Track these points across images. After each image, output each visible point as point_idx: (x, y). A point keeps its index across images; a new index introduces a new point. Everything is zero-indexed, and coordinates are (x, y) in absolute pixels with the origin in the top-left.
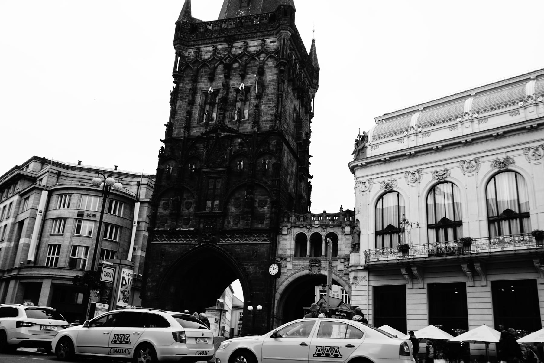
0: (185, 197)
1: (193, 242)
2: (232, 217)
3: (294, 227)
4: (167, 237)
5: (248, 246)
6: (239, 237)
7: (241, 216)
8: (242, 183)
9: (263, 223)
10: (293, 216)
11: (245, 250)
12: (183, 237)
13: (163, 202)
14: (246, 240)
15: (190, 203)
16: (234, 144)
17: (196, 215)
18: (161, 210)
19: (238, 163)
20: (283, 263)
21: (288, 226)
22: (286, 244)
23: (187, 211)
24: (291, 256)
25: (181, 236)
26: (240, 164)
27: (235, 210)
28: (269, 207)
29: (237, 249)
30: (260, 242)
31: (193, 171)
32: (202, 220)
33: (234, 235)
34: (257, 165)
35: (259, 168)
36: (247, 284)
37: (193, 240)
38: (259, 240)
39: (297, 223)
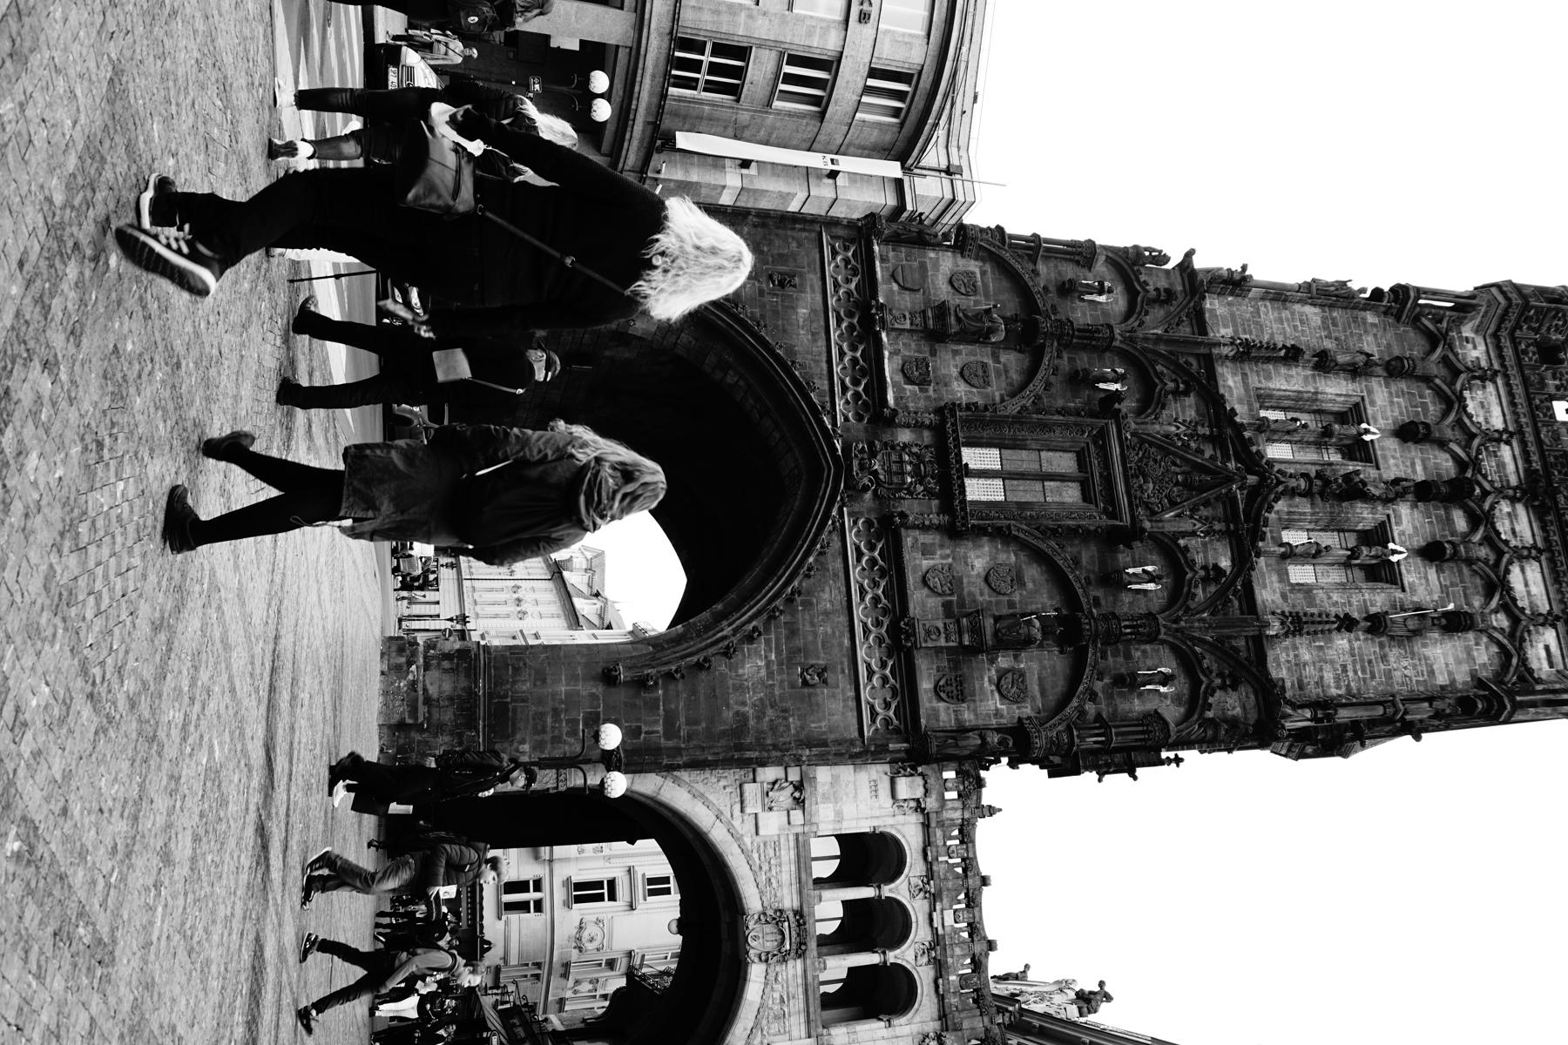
0: (1002, 360)
1: (840, 404)
2: (950, 560)
3: (923, 824)
4: (849, 294)
5: (846, 642)
6: (876, 600)
7: (954, 598)
8: (1080, 591)
9: (941, 699)
10: (967, 815)
11: (829, 630)
12: (854, 361)
13: (977, 271)
14: (866, 631)
15: (987, 383)
16: (1211, 541)
17: (946, 411)
18: (946, 263)
19: (1150, 568)
20: (784, 797)
21: (928, 800)
22: (856, 796)
23: (954, 372)
24: (812, 824)
25: (858, 354)
26: (1152, 578)
27: (974, 573)
28: (1002, 716)
29: (829, 597)
30: (865, 695)
31: (1102, 386)
32: (926, 434)
33: (881, 577)
34: (1148, 647)
35: (1138, 654)
36: (695, 659)
37: (847, 402)
38: (873, 688)
39: (939, 833)
